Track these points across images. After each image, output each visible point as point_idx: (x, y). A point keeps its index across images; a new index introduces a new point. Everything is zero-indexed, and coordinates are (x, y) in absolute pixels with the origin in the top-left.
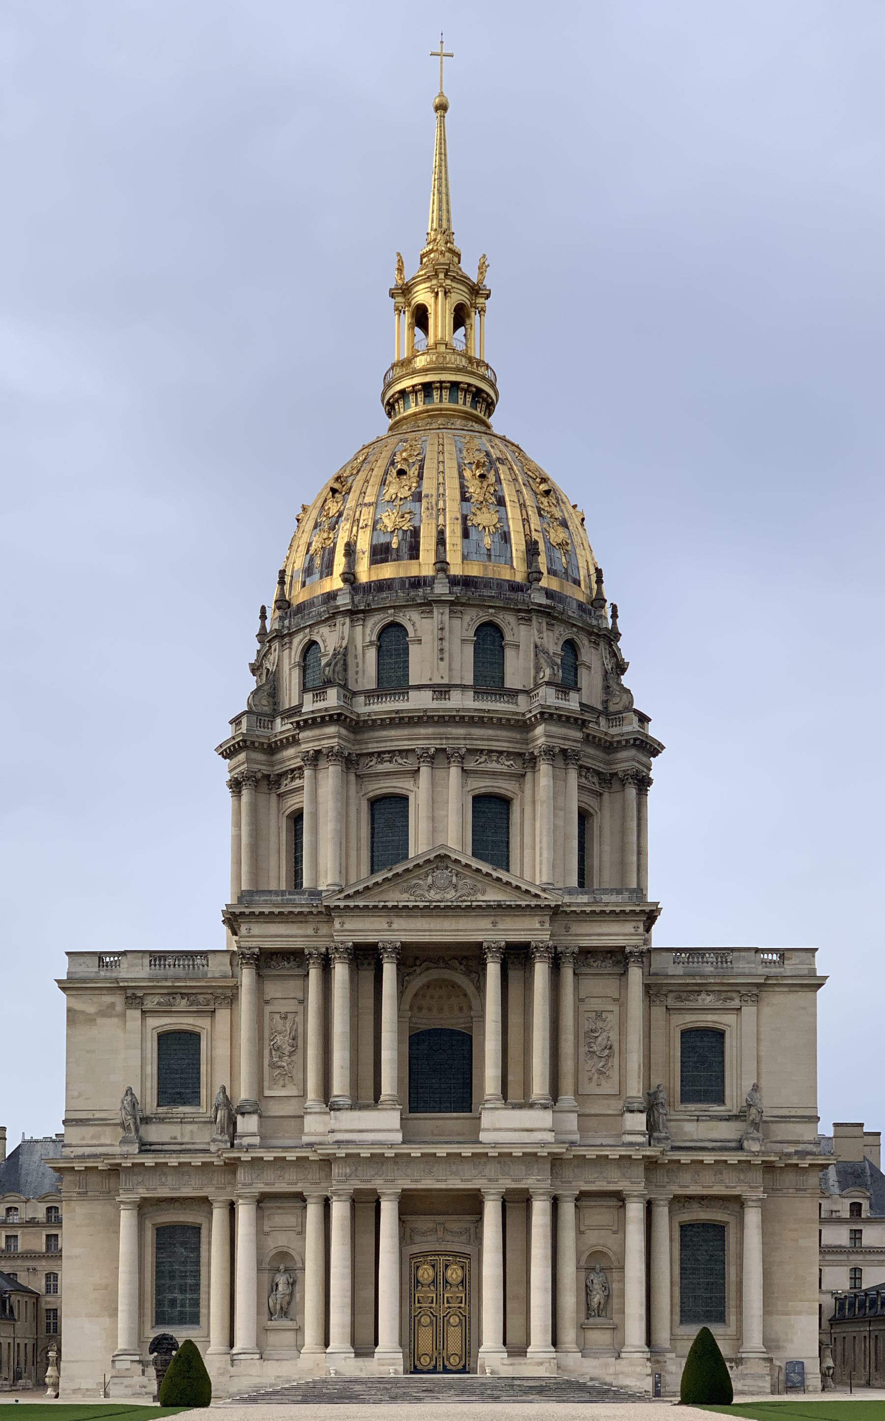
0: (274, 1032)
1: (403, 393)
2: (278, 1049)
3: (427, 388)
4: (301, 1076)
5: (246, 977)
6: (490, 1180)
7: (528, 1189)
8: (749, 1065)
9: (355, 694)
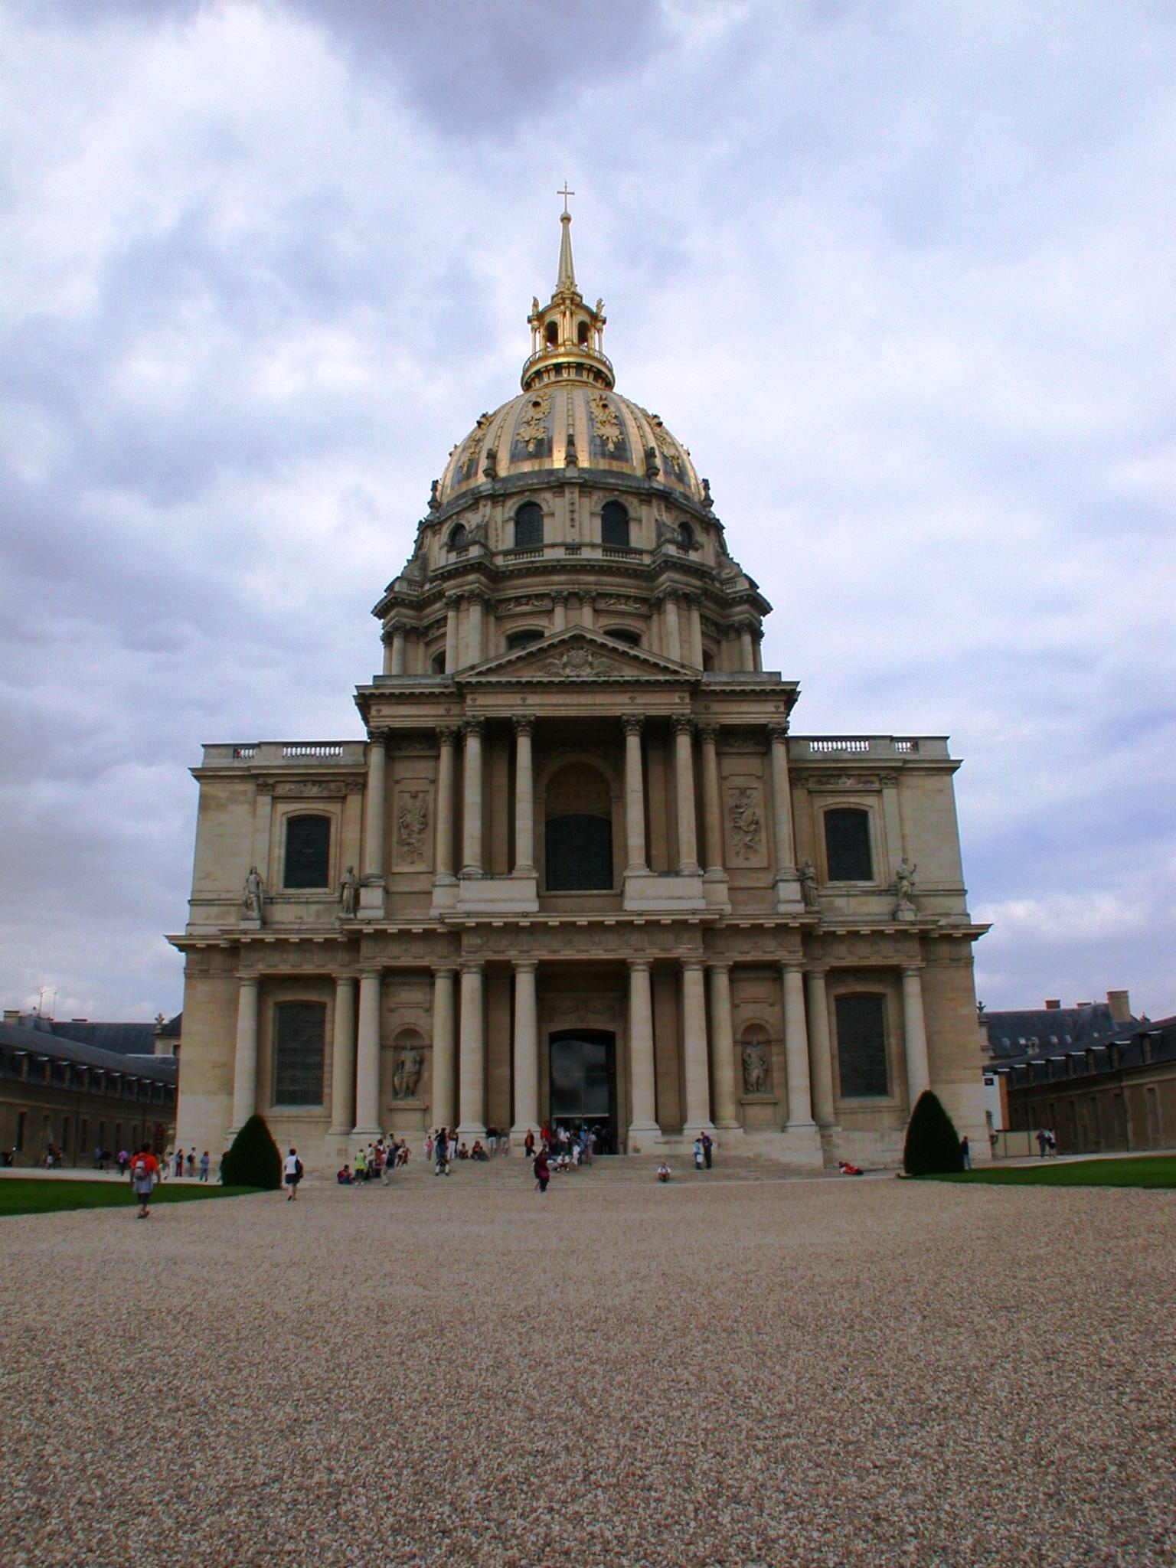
0: (404, 811)
1: (539, 374)
2: (407, 826)
3: (558, 368)
4: (430, 853)
5: (376, 756)
6: (636, 950)
7: (677, 959)
8: (894, 843)
9: (494, 555)
